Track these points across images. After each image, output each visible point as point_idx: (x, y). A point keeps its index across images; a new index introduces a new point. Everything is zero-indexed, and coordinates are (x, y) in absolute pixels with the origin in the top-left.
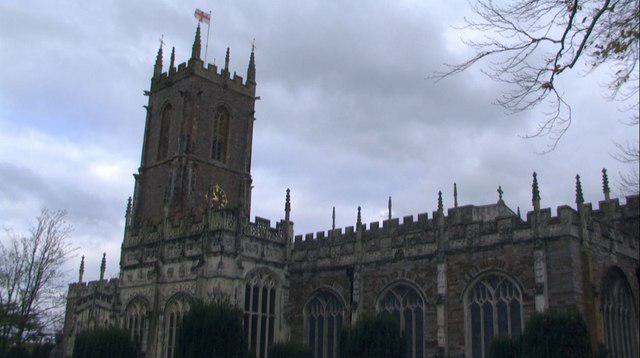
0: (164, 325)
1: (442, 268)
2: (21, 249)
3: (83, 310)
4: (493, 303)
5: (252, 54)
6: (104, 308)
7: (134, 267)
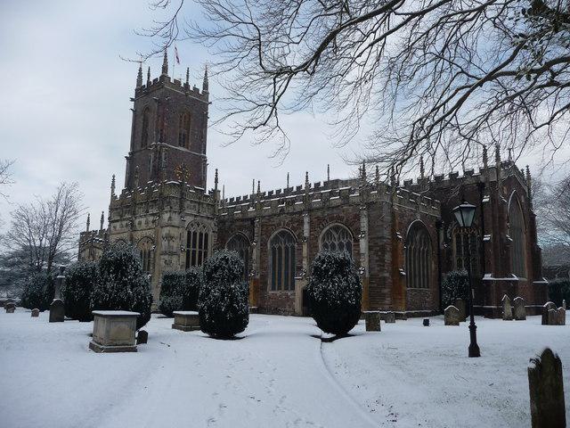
1: (306, 220)
2: (47, 209)
4: (336, 243)
7: (117, 221)
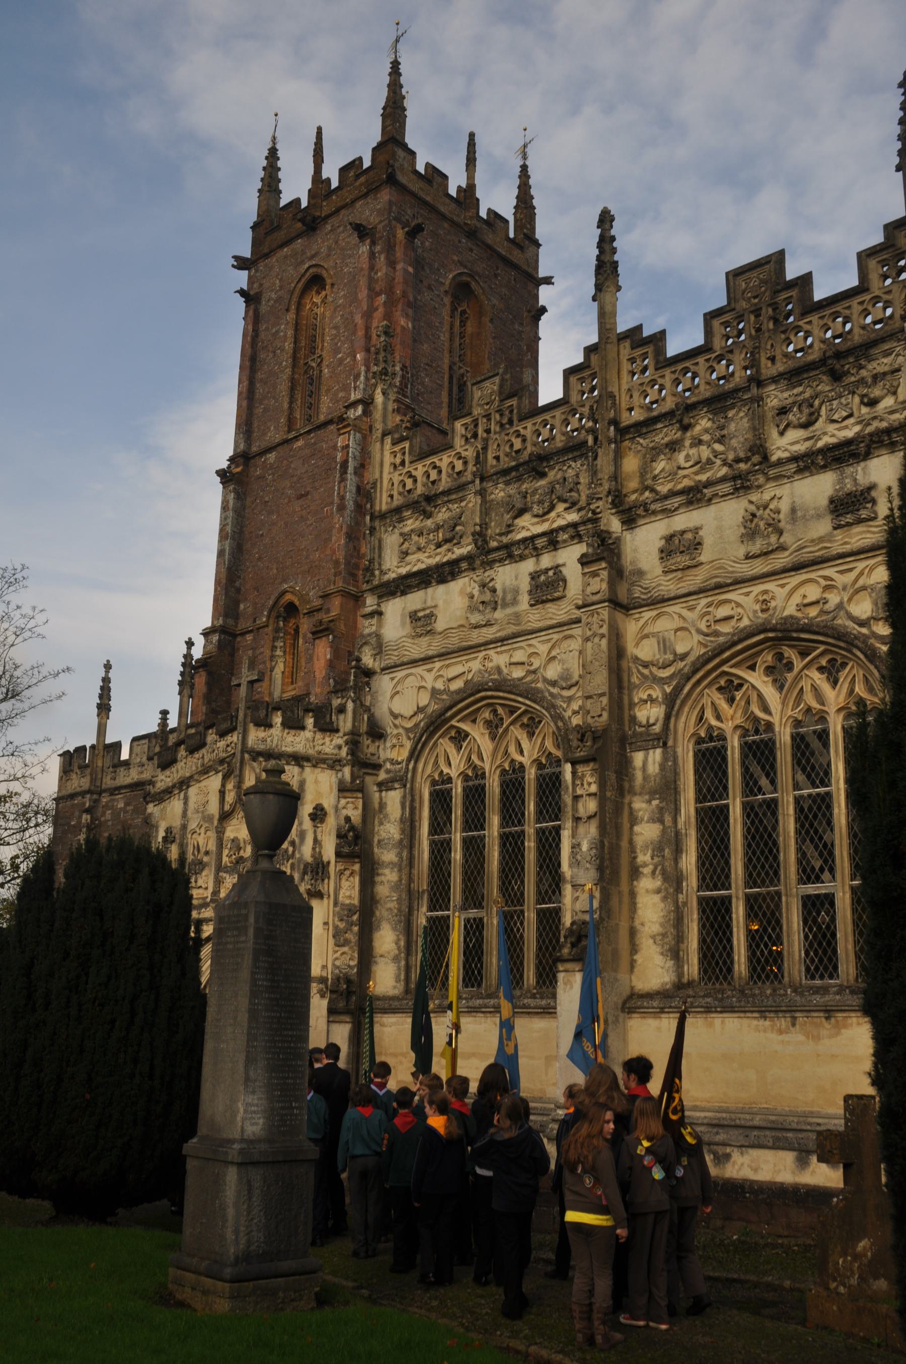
0: (667, 789)
3: (184, 784)
7: (444, 573)
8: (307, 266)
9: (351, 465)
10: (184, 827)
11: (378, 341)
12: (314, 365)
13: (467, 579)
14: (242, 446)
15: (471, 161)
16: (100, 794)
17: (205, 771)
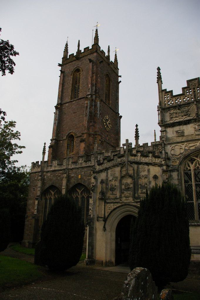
5: (116, 54)
6: (148, 164)
8: (76, 67)
9: (88, 107)
10: (107, 179)
11: (94, 82)
12: (77, 87)
13: (193, 124)
14: (60, 102)
15: (109, 51)
16: (43, 172)
17: (114, 166)
